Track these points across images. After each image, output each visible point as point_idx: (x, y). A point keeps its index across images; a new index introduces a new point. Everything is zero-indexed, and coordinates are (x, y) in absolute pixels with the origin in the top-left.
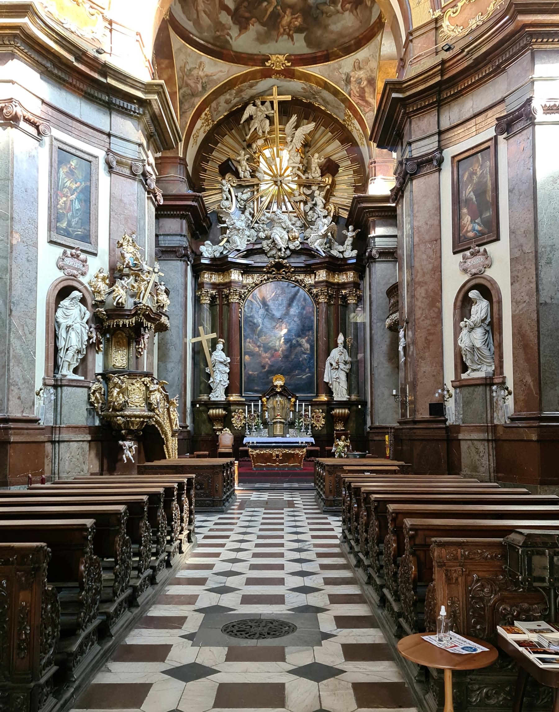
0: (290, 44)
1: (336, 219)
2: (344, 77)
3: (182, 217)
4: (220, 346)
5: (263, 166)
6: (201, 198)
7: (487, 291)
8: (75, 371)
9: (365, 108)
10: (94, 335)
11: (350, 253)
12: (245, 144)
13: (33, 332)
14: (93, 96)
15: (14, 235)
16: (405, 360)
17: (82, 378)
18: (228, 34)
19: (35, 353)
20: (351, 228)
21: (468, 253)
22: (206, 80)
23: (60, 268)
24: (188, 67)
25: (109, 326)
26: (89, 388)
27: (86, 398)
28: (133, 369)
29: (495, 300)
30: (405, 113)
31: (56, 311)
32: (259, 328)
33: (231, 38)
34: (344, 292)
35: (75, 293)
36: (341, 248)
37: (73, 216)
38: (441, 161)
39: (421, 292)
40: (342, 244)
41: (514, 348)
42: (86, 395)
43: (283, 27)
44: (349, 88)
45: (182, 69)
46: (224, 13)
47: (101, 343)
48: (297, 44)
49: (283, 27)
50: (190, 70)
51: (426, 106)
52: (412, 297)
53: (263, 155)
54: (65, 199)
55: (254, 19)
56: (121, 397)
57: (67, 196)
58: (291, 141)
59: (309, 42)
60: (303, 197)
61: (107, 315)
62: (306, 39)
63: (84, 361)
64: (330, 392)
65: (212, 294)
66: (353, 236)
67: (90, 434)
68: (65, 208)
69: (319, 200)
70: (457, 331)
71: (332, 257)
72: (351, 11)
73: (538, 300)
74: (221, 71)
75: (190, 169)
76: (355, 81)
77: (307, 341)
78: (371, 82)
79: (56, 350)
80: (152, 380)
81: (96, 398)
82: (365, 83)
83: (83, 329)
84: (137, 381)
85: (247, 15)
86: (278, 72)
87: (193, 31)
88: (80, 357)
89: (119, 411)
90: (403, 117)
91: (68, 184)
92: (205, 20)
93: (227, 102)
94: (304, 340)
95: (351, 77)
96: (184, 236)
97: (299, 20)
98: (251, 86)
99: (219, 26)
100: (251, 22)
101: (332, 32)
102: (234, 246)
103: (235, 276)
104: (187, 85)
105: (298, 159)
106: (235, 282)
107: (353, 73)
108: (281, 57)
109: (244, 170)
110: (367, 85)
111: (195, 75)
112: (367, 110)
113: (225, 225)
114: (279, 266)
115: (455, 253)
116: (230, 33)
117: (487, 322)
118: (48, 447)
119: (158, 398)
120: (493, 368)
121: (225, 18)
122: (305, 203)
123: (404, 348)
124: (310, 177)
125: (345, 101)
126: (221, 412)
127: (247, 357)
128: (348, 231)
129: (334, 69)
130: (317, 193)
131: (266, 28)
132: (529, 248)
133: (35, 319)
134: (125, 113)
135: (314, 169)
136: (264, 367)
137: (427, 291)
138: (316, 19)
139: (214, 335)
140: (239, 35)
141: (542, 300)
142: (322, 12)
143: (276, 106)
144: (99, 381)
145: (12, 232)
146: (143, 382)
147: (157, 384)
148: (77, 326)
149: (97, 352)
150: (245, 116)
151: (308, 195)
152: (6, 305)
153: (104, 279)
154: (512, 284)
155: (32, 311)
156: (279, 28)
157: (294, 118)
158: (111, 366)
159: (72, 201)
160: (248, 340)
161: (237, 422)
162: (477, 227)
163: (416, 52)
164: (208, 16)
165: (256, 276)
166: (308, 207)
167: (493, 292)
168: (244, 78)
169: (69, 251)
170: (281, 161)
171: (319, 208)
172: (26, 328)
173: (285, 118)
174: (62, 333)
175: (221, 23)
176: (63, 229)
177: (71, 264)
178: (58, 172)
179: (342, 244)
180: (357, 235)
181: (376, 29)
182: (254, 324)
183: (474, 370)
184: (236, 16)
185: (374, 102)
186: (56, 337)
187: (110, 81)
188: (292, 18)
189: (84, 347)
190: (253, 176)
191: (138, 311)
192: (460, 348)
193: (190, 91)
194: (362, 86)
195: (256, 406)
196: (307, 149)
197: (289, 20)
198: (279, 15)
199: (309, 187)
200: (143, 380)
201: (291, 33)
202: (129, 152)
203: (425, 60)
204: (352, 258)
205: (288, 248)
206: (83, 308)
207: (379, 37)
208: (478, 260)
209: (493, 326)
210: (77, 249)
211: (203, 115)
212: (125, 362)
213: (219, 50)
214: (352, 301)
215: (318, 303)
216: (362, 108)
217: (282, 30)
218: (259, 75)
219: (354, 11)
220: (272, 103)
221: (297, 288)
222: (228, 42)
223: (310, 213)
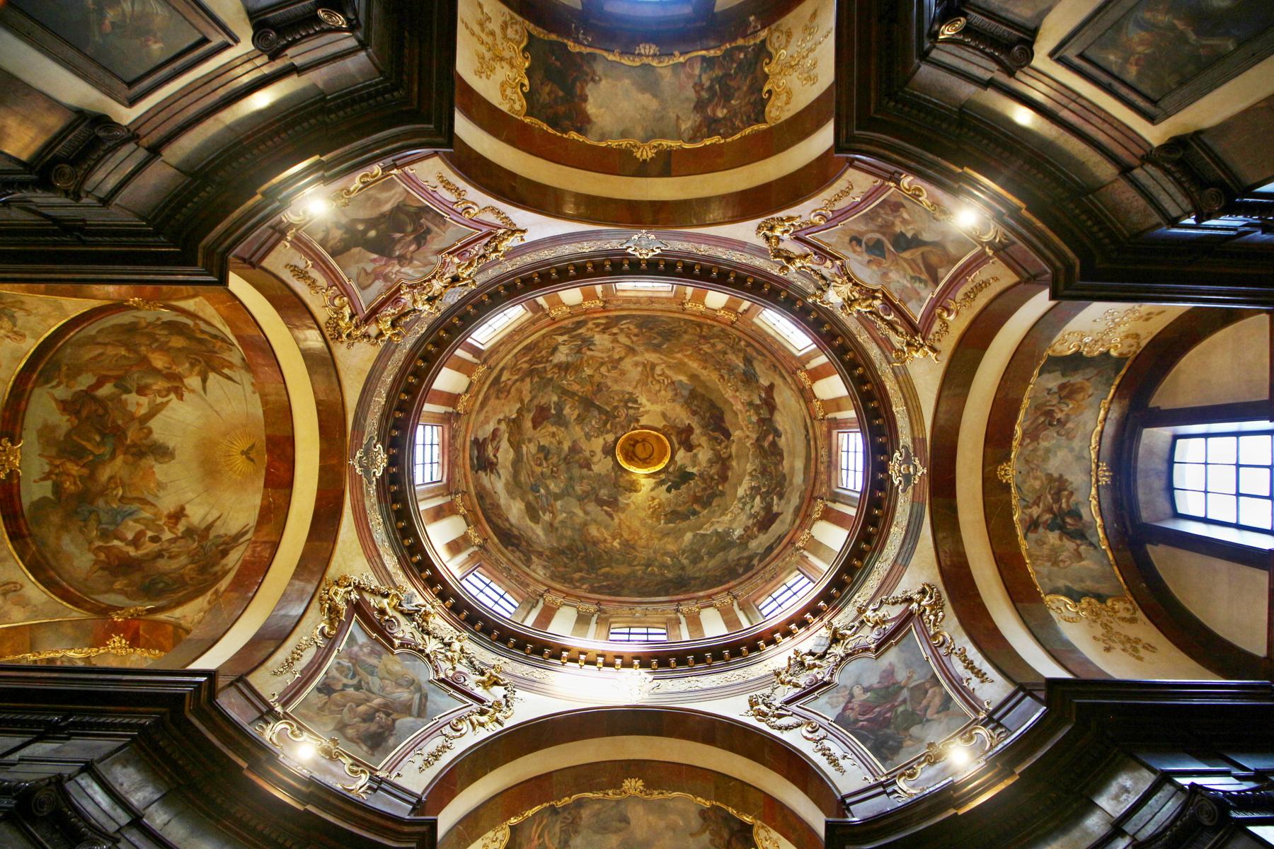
0: (36, 475)
18: (59, 384)
24: (19, 314)
33: (53, 387)
46: (93, 380)
48: (35, 487)
59: (41, 504)
72: (96, 562)
85: (84, 413)
92: (89, 354)
97: (73, 487)
101: (58, 538)
121: (85, 381)
138: (76, 513)
140: (55, 400)
156: (59, 457)
184: (88, 394)
197: (74, 473)
198: (81, 458)
201: (54, 477)
202: (106, 176)
217: (57, 462)
219: (97, 567)
222: (47, 382)
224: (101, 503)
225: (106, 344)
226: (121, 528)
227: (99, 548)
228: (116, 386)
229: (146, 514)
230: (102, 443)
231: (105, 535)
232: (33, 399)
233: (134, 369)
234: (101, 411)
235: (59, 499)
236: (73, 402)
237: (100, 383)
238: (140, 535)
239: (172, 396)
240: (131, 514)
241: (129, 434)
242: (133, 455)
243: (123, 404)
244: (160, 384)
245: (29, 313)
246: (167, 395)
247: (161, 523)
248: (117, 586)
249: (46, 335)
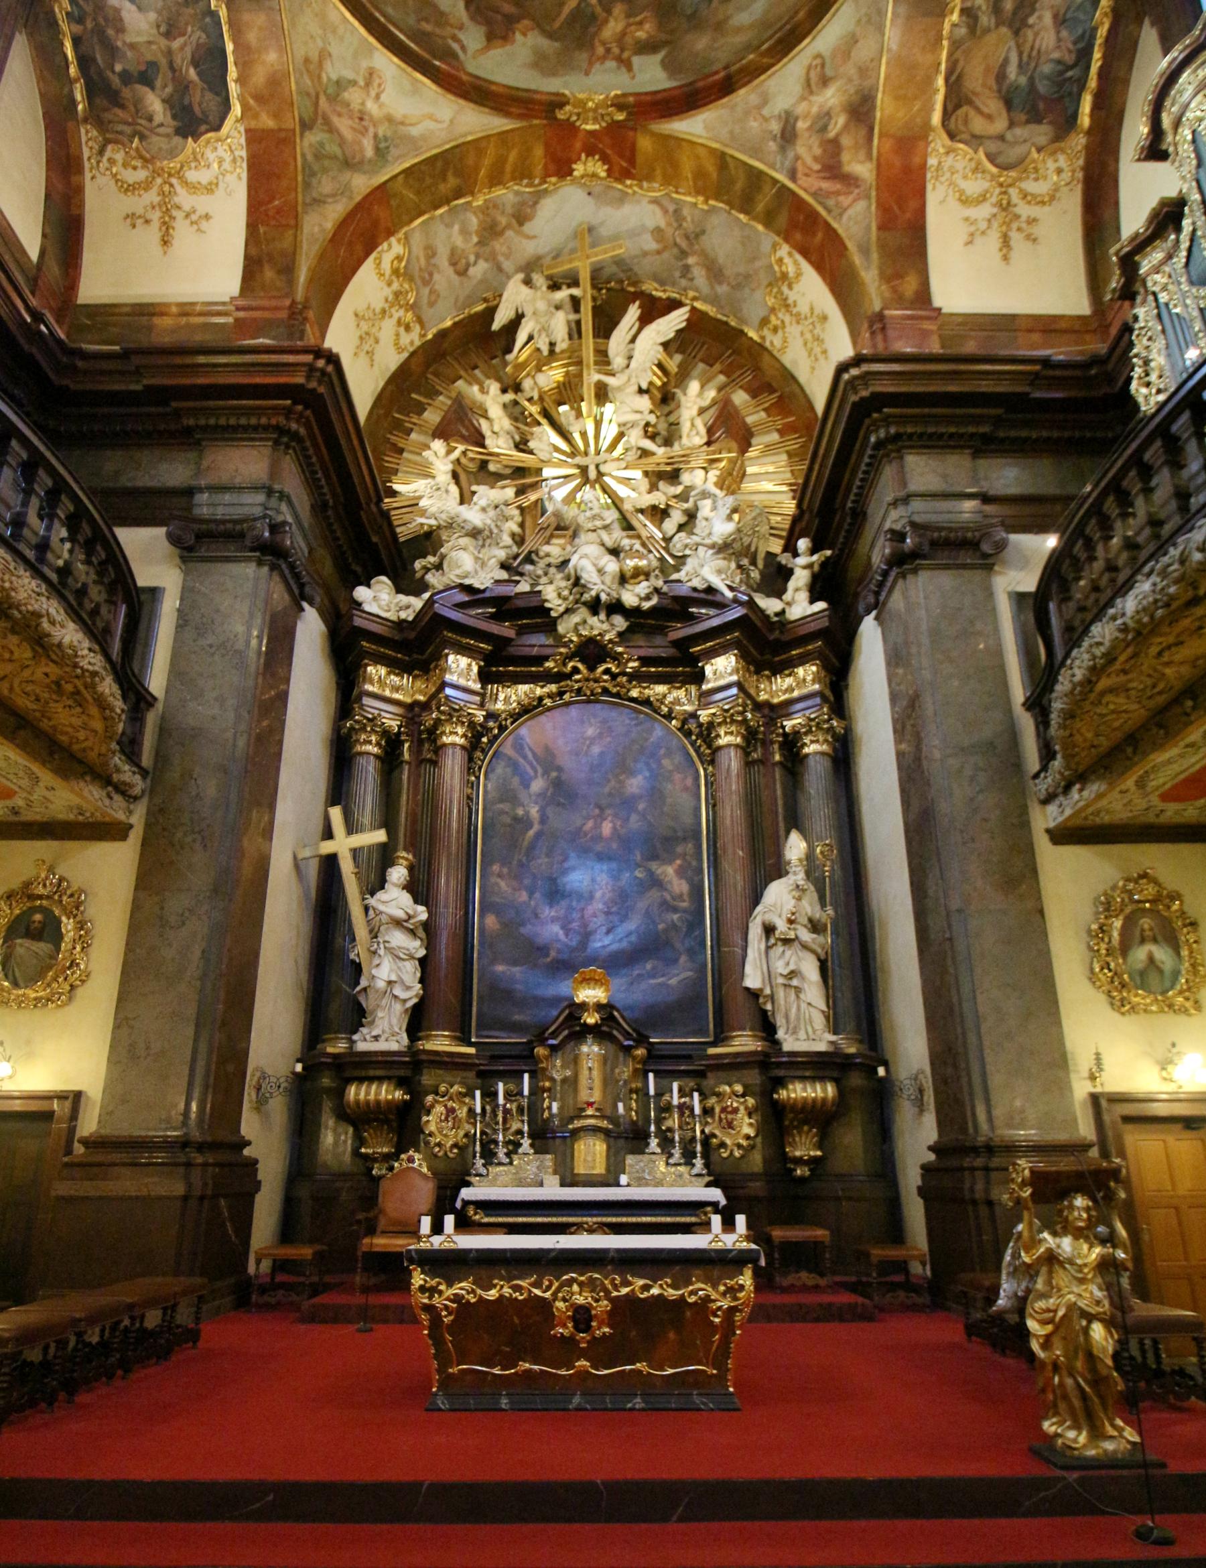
2: (775, 127)
9: (841, 198)
20: (803, 544)
22: (389, 134)
24: (332, 71)
32: (531, 833)
34: (789, 724)
43: (604, 43)
44: (791, 155)
49: (604, 43)
55: (526, 22)
62: (665, 65)
66: (809, 566)
74: (431, 117)
76: (810, 128)
77: (680, 873)
82: (841, 120)
85: (508, 8)
94: (670, 870)
95: (796, 119)
97: (647, 26)
100: (519, 26)
104: (331, 129)
107: (804, 105)
110: (846, 127)
111: (355, 106)
112: (845, 200)
116: (461, 36)
128: (796, 555)
129: (747, 113)
131: (557, 45)
157: (633, 312)
188: (629, 25)
194: (831, 134)
198: (594, 17)
216: (831, 202)
217: (600, 50)
222: (454, 56)
235: (666, 43)
236: (488, 23)
249: (362, 30)
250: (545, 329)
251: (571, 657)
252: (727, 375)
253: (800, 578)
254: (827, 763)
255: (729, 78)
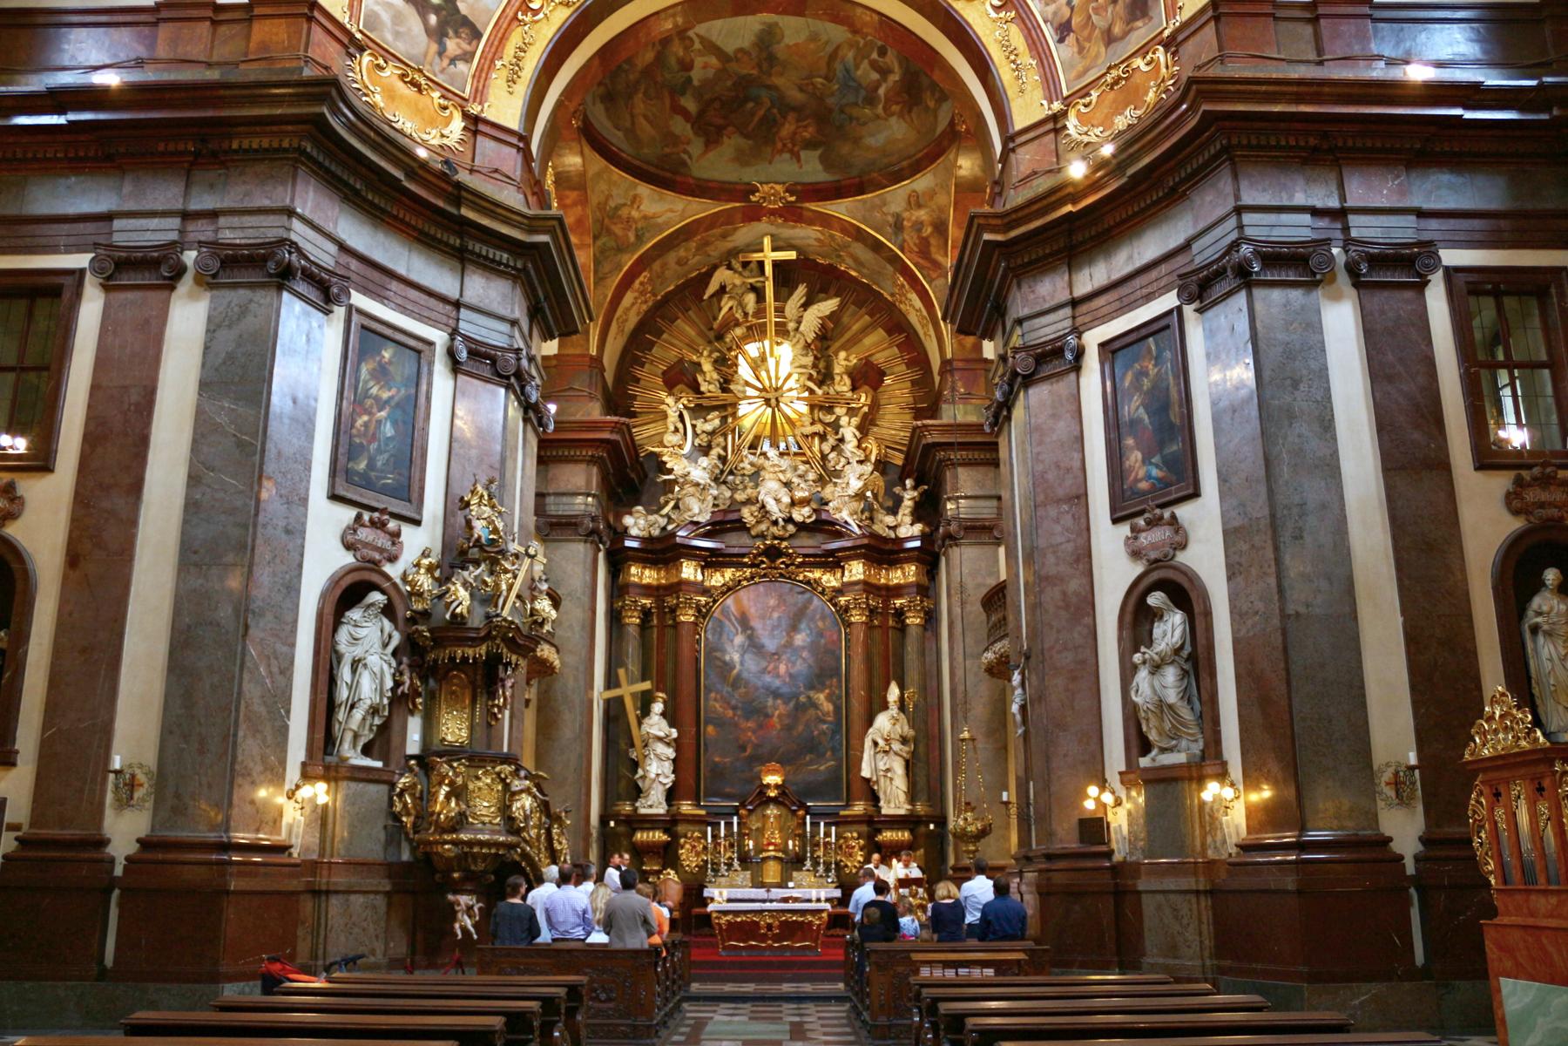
0: (794, 167)
1: (882, 466)
2: (890, 219)
3: (592, 461)
4: (658, 707)
5: (744, 371)
6: (628, 426)
7: (1184, 593)
8: (367, 751)
10: (406, 678)
11: (909, 530)
12: (711, 335)
13: (287, 670)
14: (434, 238)
15: (265, 483)
16: (1026, 733)
17: (379, 764)
19: (288, 712)
20: (909, 483)
21: (1141, 522)
23: (348, 546)
24: (612, 204)
25: (435, 661)
26: (393, 785)
27: (385, 805)
28: (480, 748)
29: (1197, 609)
30: (1007, 269)
31: (335, 630)
34: (898, 602)
35: (376, 597)
36: (890, 520)
37: (379, 451)
38: (1080, 353)
39: (1052, 595)
40: (894, 511)
41: (1241, 704)
42: (386, 798)
45: (601, 207)
47: (419, 695)
48: (807, 168)
50: (617, 208)
51: (1046, 257)
52: (1033, 608)
53: (744, 353)
54: (365, 418)
55: (730, 129)
56: (453, 804)
57: (370, 414)
58: (797, 329)
60: (819, 428)
61: (433, 639)
63: (384, 729)
64: (874, 798)
65: (643, 606)
67: (389, 877)
68: (365, 434)
69: (849, 432)
70: (1128, 673)
71: (874, 536)
72: (901, 115)
73: (1282, 610)
74: (672, 211)
75: (609, 376)
77: (829, 698)
78: (940, 228)
79: (331, 707)
80: (517, 770)
81: (405, 804)
83: (386, 667)
84: (485, 774)
85: (721, 122)
86: (773, 213)
87: (624, 146)
88: (377, 721)
89: (444, 831)
90: (1004, 277)
91: (374, 391)
93: (680, 262)
94: (822, 696)
96: (594, 496)
98: (724, 236)
99: (672, 139)
102: (687, 516)
103: (689, 571)
104: (610, 232)
105: (809, 360)
106: (687, 583)
108: (779, 188)
109: (709, 380)
112: (934, 275)
113: (671, 477)
114: (773, 553)
115: (1115, 521)
116: (689, 149)
117: (1185, 653)
118: (307, 905)
119: (527, 807)
120: (1201, 744)
121: (680, 127)
122: (823, 438)
123: (1023, 708)
124: (832, 391)
125: (894, 260)
126: (659, 836)
127: (710, 729)
128: (905, 489)
130: (844, 421)
132: (1260, 509)
133: (293, 645)
134: (491, 268)
135: (837, 378)
136: (743, 748)
137: (1064, 593)
139: (647, 685)
141: (1291, 609)
142: (851, 119)
143: (768, 269)
144: (411, 770)
145: (260, 477)
146: (498, 774)
147: (526, 778)
148: (374, 660)
149: (412, 713)
150: (713, 287)
151: (828, 424)
152: (238, 617)
153: (430, 569)
154: (1229, 578)
155: (288, 628)
156: (774, 143)
157: (801, 290)
158: (436, 741)
159: (379, 422)
160: (713, 695)
161: (689, 858)
162: (1155, 472)
163: (1022, 168)
164: (650, 122)
165: (729, 573)
166: (826, 447)
167: (1193, 595)
168: (712, 221)
169: (366, 516)
170: (777, 363)
171: (850, 446)
172: (274, 662)
173: (785, 291)
174: (345, 673)
175: (672, 135)
176: (358, 473)
177: (370, 538)
178: (357, 370)
179: (894, 511)
180: (921, 495)
181: (945, 143)
182: (725, 663)
183: (1163, 750)
185: (949, 262)
186: (332, 681)
187: (464, 212)
189: (386, 701)
190: (725, 390)
191: (494, 630)
192: (1135, 705)
193: (613, 244)
195: (729, 825)
196: (826, 344)
197: (793, 127)
198: (775, 121)
199: (830, 410)
200: (498, 769)
202: (493, 334)
203: (1040, 180)
204: (911, 538)
205: (789, 520)
206: (387, 625)
207: (952, 156)
208: (1160, 535)
209: (1196, 661)
210: (383, 511)
211: (637, 284)
212: (464, 734)
213: (667, 175)
214: (913, 620)
215: (849, 625)
217: (779, 145)
218: (739, 216)
220: (761, 264)
221: (807, 595)
222: (684, 164)
223: (832, 455)
224: (831, 101)
225: (632, 116)
226: (865, 83)
227: (885, 109)
228: (683, 94)
229: (850, 55)
230: (757, 100)
231: (871, 100)
232: (706, 175)
233: (659, 79)
234: (717, 105)
237: (685, 113)
238: (874, 65)
239: (691, 33)
240: (847, 71)
241: (745, 72)
242: (771, 67)
243: (706, 83)
244: (677, 49)
245: (609, 197)
246: (691, 39)
247: (862, 42)
248: (931, 104)
250: (742, 305)
251: (760, 555)
252: (871, 316)
253: (907, 504)
254: (920, 630)
255: (862, 183)
